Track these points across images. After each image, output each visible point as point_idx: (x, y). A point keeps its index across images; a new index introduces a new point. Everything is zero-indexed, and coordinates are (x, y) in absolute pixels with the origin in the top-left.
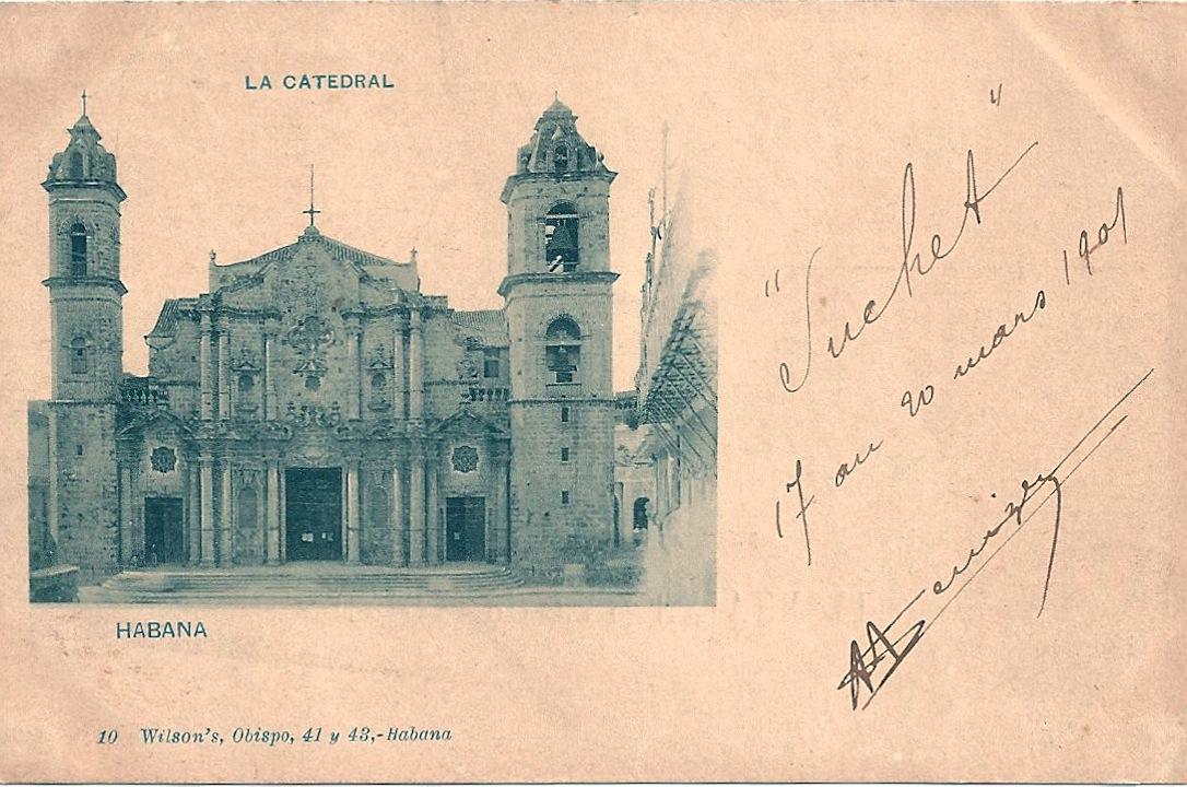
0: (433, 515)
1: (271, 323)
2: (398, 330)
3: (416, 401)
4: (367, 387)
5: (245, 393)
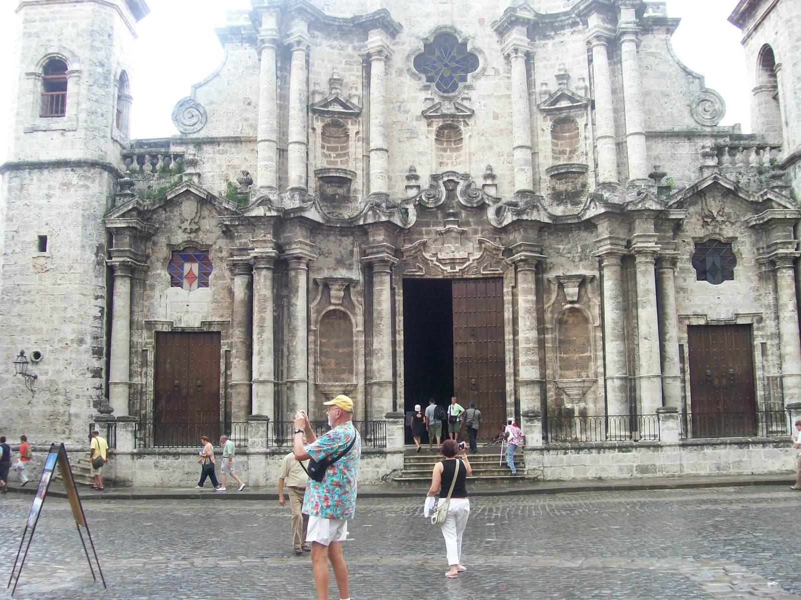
0: (672, 350)
1: (376, 39)
2: (598, 37)
3: (636, 148)
4: (545, 139)
5: (333, 155)
